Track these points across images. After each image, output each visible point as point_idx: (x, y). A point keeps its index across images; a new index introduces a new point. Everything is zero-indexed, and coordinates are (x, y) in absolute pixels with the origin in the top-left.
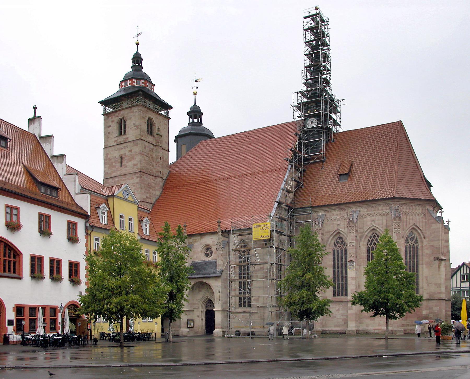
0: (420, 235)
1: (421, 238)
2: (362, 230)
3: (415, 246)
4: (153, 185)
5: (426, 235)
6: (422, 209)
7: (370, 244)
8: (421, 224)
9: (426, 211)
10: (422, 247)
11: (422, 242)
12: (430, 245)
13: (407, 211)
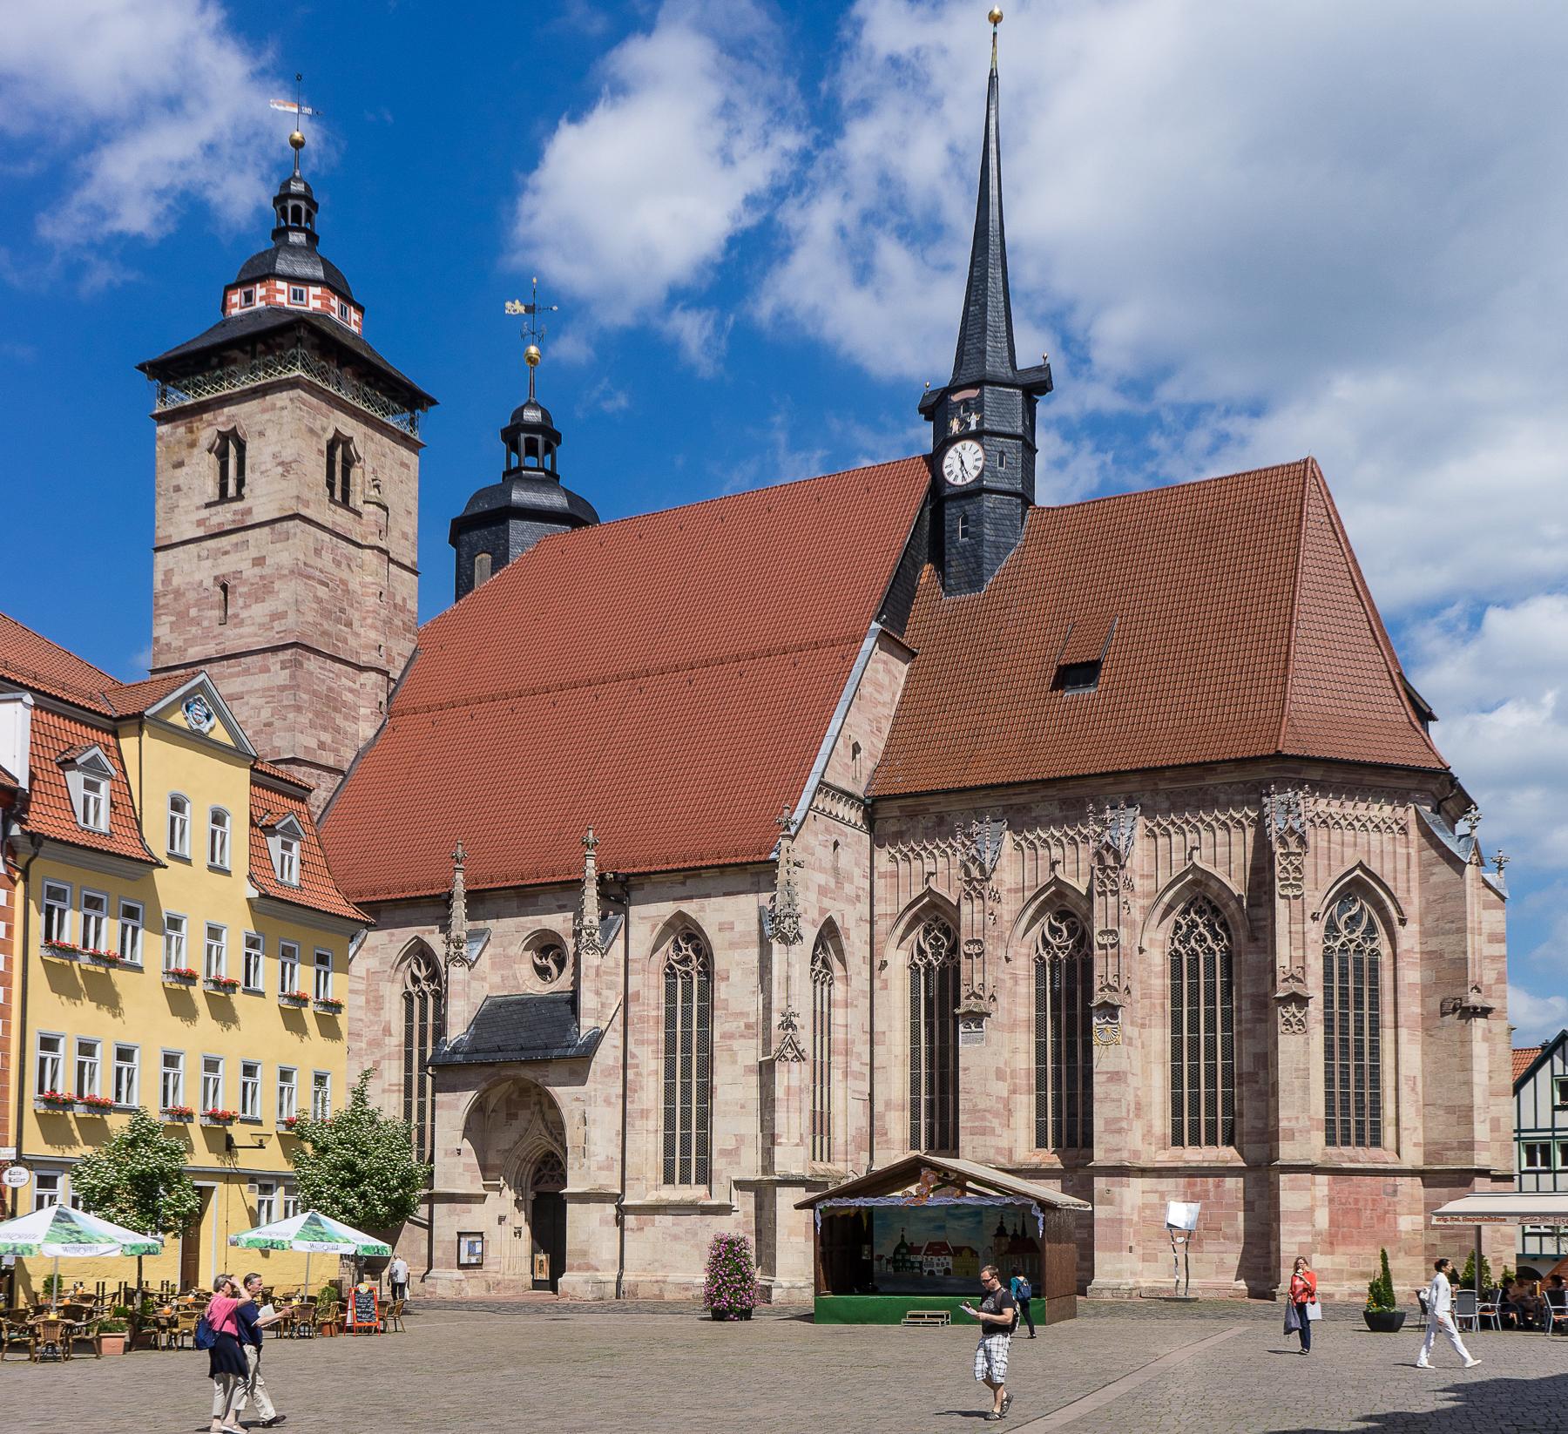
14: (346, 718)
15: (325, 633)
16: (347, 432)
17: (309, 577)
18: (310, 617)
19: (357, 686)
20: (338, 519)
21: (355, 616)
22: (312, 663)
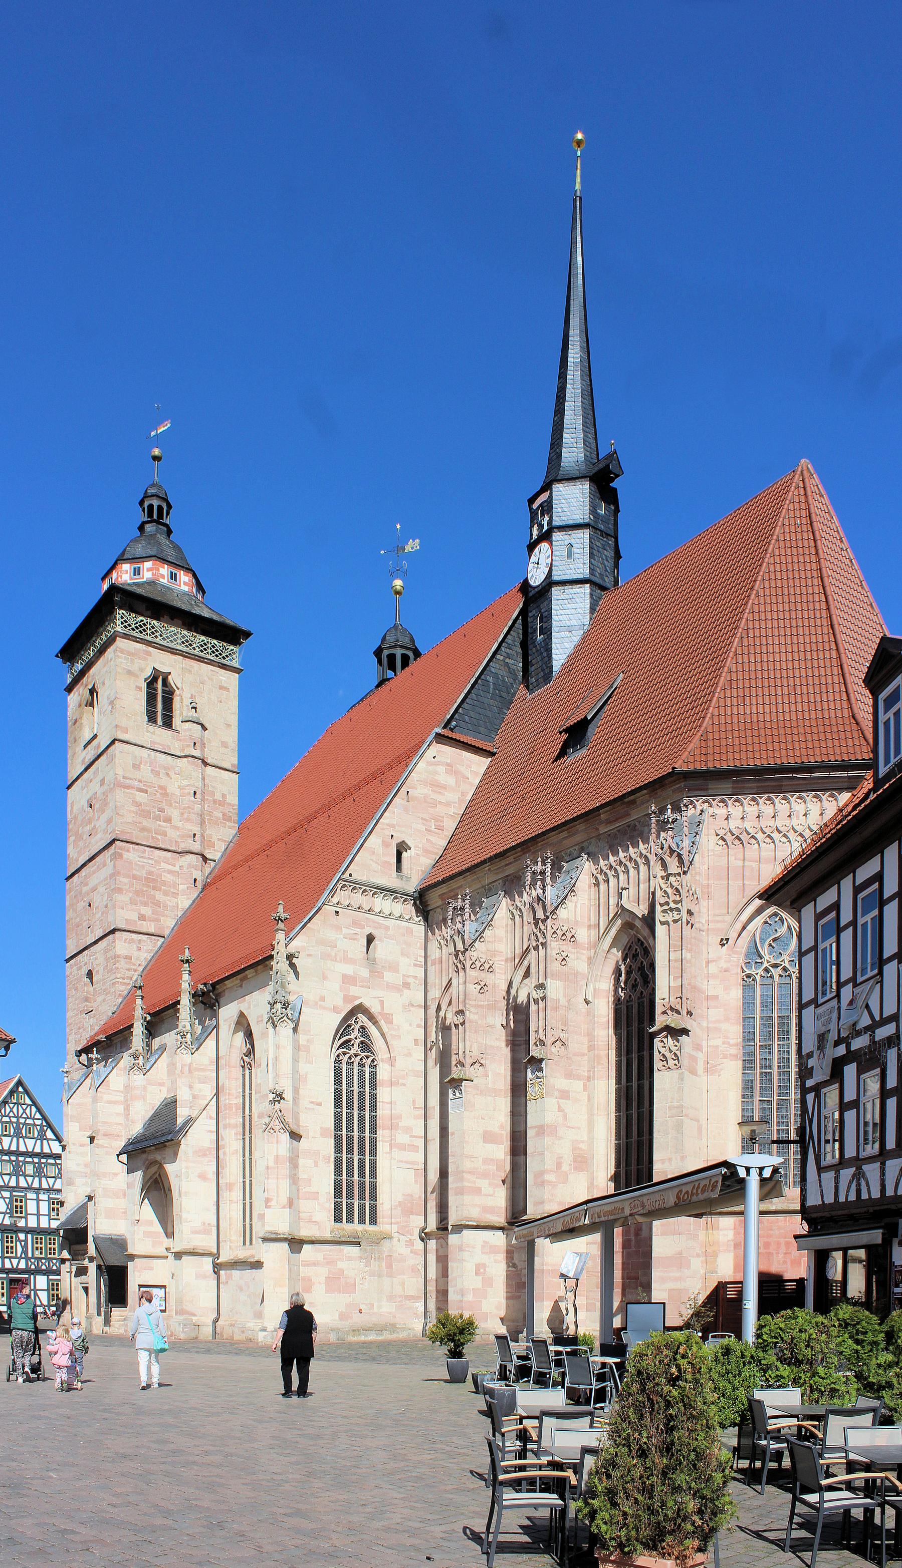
4: (168, 878)
14: (166, 893)
17: (128, 787)
19: (177, 868)
21: (175, 814)
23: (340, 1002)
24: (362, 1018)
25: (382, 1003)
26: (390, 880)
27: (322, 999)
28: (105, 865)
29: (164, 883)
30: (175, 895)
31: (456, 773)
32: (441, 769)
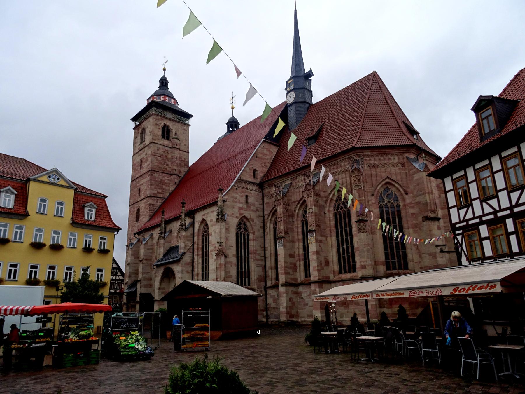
0: (399, 190)
1: (402, 194)
2: (326, 194)
3: (395, 205)
4: (167, 181)
5: (409, 190)
6: (399, 158)
7: (337, 210)
8: (399, 177)
9: (405, 160)
10: (405, 205)
11: (404, 199)
12: (416, 201)
13: (376, 162)
14: (166, 186)
15: (160, 167)
16: (168, 124)
18: (155, 164)
20: (165, 143)
21: (169, 163)
22: (156, 175)
23: (238, 215)
24: (245, 220)
25: (250, 215)
26: (251, 179)
27: (233, 214)
28: (146, 177)
29: (166, 183)
30: (169, 186)
31: (269, 151)
32: (265, 150)
